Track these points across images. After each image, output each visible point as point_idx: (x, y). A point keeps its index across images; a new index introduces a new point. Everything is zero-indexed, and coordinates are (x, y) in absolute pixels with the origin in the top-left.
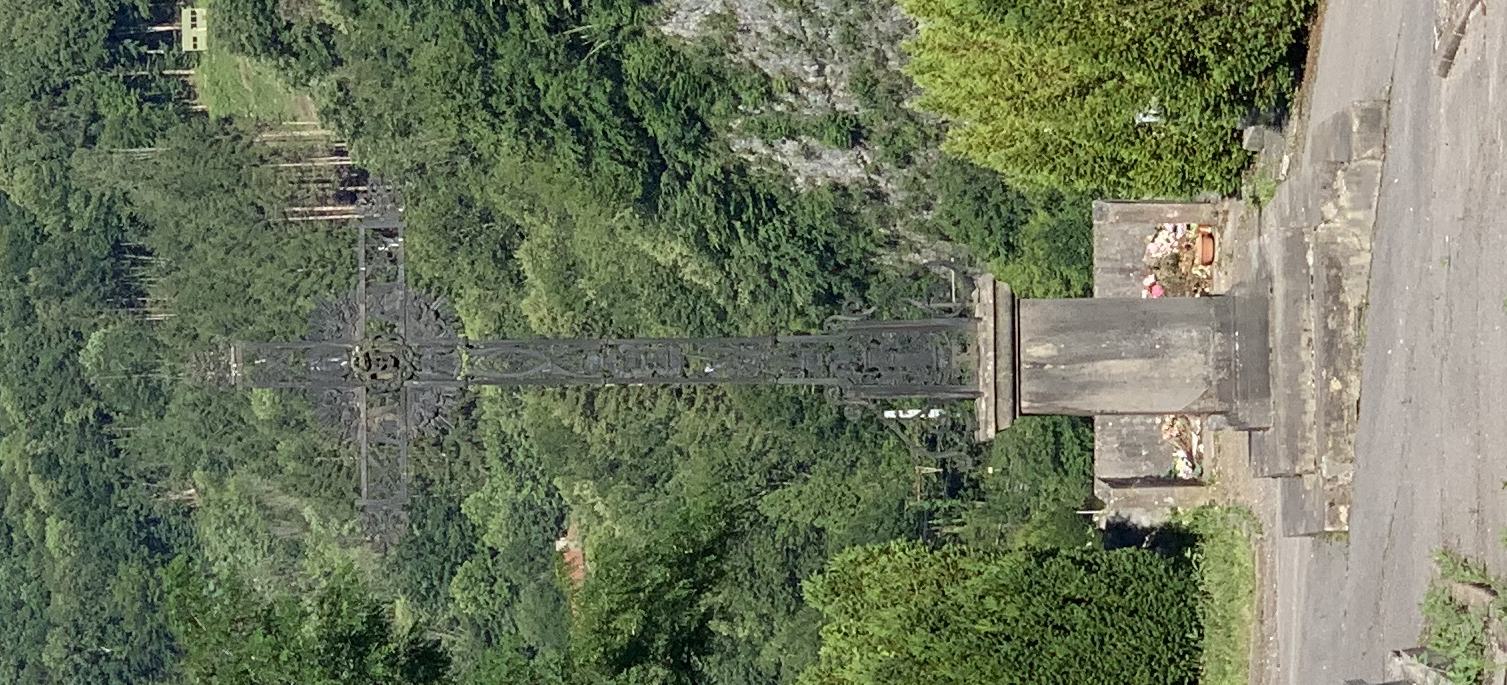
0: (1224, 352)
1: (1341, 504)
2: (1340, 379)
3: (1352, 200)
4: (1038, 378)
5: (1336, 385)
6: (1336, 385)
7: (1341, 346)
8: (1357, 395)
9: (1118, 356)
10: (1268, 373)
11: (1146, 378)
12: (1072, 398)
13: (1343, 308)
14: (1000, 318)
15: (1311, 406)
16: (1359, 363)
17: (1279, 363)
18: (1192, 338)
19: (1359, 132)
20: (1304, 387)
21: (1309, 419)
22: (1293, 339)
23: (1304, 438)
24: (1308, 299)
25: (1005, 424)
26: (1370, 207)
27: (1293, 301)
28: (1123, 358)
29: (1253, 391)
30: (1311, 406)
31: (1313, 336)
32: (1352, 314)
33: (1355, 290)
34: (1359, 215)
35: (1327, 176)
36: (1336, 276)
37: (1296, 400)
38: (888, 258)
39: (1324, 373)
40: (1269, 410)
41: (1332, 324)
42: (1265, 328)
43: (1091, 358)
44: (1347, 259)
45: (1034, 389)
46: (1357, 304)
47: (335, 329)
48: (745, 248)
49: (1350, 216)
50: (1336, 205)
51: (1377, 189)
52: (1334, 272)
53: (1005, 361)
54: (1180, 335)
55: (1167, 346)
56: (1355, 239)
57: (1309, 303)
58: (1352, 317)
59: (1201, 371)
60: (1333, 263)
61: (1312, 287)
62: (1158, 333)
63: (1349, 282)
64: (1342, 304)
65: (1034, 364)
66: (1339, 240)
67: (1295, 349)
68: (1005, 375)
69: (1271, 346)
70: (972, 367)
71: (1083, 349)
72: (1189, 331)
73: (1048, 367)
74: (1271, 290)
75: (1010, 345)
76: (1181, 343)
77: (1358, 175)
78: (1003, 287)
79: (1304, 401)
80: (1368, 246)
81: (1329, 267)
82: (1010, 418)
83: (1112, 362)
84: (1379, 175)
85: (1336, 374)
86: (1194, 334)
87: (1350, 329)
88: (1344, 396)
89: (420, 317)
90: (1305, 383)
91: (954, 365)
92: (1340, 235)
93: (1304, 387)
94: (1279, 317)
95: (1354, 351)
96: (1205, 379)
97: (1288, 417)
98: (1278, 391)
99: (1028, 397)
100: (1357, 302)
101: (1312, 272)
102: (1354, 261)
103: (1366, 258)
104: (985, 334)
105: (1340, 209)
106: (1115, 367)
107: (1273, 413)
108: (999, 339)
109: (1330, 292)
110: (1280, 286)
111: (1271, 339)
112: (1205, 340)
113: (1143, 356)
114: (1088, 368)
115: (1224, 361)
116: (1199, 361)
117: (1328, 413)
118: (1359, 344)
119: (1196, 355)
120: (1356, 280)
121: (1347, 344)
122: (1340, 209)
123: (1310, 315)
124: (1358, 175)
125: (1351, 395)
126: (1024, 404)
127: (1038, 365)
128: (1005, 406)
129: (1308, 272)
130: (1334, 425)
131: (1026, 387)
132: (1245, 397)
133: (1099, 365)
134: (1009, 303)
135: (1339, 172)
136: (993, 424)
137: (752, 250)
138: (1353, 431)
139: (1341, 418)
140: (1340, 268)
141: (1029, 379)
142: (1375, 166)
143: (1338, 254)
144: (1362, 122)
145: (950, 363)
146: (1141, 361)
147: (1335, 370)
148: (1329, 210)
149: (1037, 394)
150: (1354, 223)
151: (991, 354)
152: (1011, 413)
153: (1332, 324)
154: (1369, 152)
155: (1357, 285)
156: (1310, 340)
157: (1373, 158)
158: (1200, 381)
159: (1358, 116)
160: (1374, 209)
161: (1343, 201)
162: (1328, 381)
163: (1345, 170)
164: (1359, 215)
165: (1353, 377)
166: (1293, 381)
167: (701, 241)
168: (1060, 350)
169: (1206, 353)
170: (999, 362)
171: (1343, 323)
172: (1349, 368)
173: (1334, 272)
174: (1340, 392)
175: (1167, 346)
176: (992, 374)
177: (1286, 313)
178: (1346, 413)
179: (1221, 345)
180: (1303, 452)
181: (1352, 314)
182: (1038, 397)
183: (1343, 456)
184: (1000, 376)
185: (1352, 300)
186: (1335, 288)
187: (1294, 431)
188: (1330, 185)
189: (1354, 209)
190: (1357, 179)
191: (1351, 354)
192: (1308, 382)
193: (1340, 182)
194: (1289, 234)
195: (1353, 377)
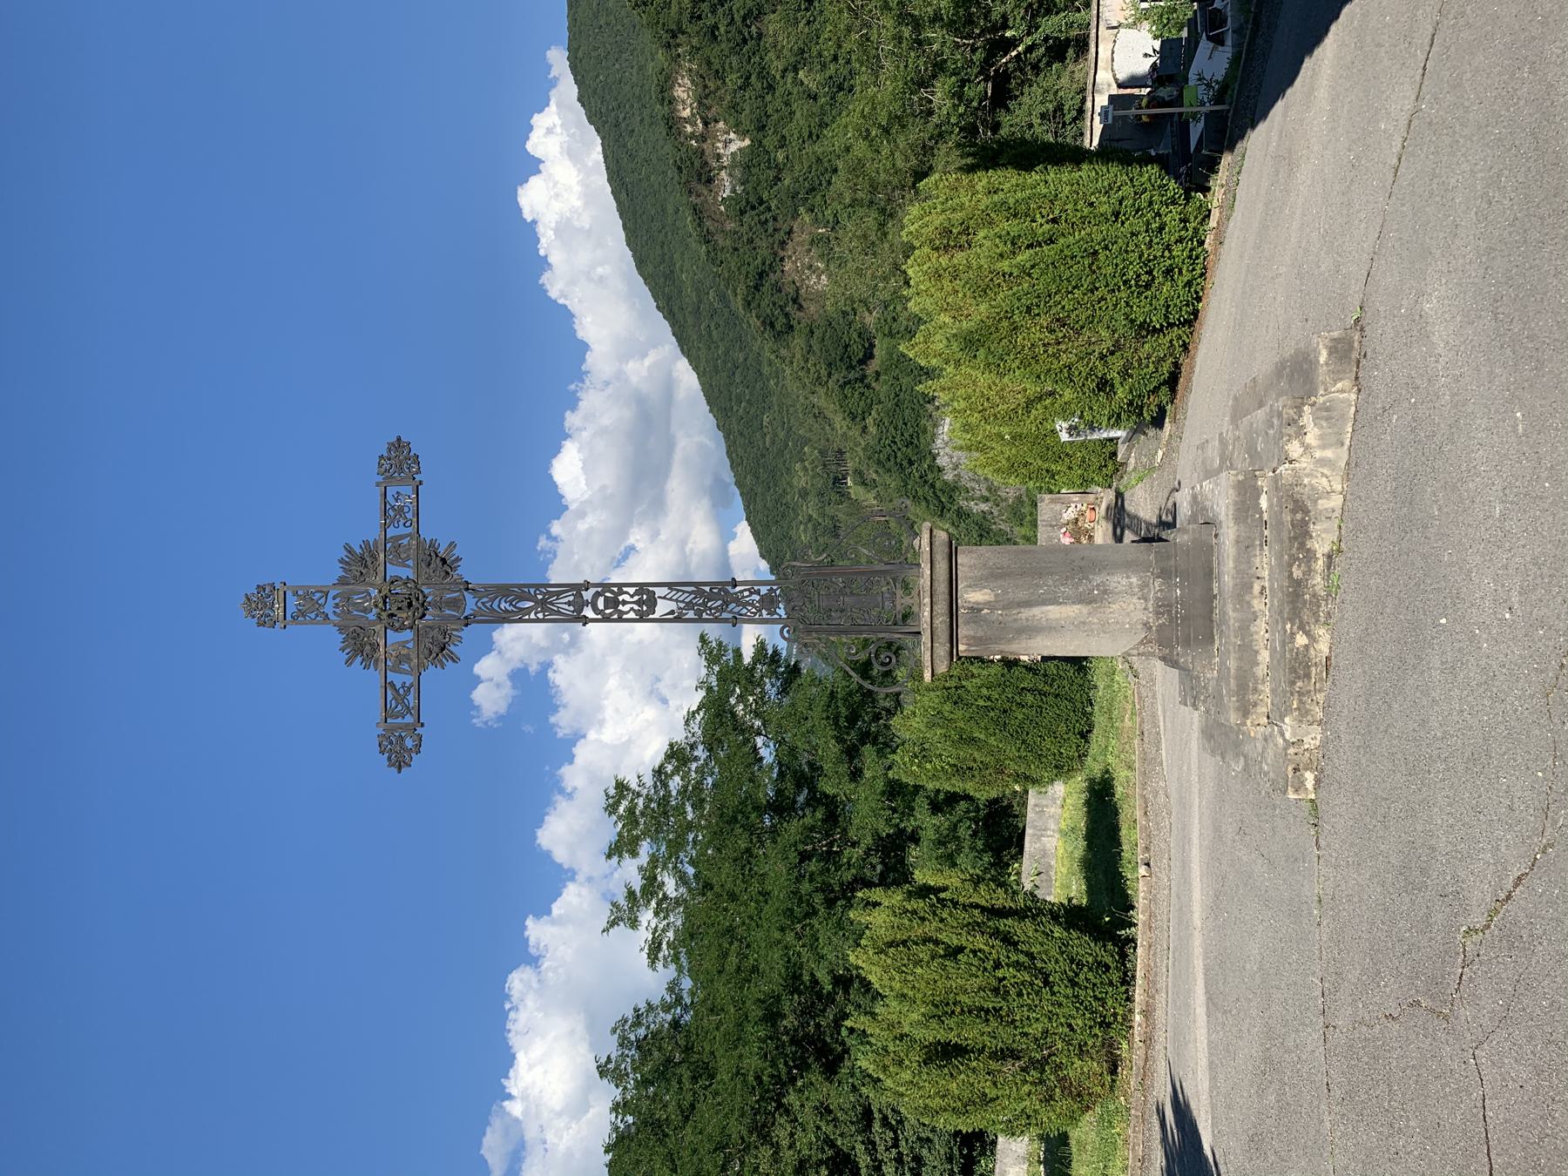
0: (1165, 598)
1: (1306, 770)
2: (1308, 634)
3: (1321, 437)
4: (975, 622)
5: (1301, 640)
6: (1301, 640)
7: (1307, 597)
8: (1326, 651)
9: (1054, 601)
10: (1212, 621)
11: (1084, 623)
12: (1010, 641)
13: (1310, 556)
14: (937, 566)
15: (1264, 657)
16: (1329, 615)
17: (1231, 613)
18: (1131, 584)
19: (1327, 364)
20: (1256, 637)
21: (1261, 671)
22: (1244, 587)
23: (1255, 690)
24: (1261, 545)
25: (942, 668)
26: (1342, 444)
27: (1245, 548)
28: (1061, 603)
29: (1196, 638)
30: (1264, 657)
31: (1267, 585)
32: (1320, 562)
33: (1323, 535)
34: (1329, 454)
35: (1291, 412)
36: (1303, 519)
37: (1247, 652)
39: (1288, 626)
40: (1214, 657)
41: (1297, 573)
42: (1209, 574)
43: (1028, 604)
44: (1315, 502)
45: (972, 633)
46: (1326, 551)
47: (358, 574)
49: (1318, 454)
50: (1302, 444)
51: (1350, 424)
52: (1299, 516)
53: (942, 607)
54: (1119, 581)
55: (1105, 592)
56: (1324, 479)
57: (1262, 549)
58: (1320, 564)
59: (1141, 616)
60: (1299, 506)
61: (1266, 533)
62: (1098, 580)
63: (1317, 527)
64: (1309, 550)
65: (972, 608)
66: (1306, 481)
67: (1247, 598)
68: (941, 621)
69: (1215, 592)
70: (915, 609)
71: (1022, 595)
72: (1128, 577)
73: (985, 611)
74: (1216, 536)
75: (947, 591)
76: (1120, 588)
77: (1327, 409)
78: (942, 536)
79: (1257, 652)
80: (1339, 488)
81: (1294, 511)
82: (946, 663)
83: (1050, 607)
84: (1353, 409)
85: (1302, 628)
86: (1134, 580)
87: (1318, 579)
88: (1312, 652)
89: (429, 564)
90: (1257, 633)
91: (899, 607)
92: (1308, 475)
93: (1256, 637)
94: (1230, 564)
95: (1323, 603)
96: (1145, 625)
97: (1239, 668)
99: (965, 641)
100: (1326, 549)
101: (1265, 516)
102: (1323, 504)
103: (1336, 501)
105: (1307, 448)
106: (1054, 612)
107: (1217, 659)
108: (936, 584)
109: (1295, 538)
110: (1229, 534)
111: (1215, 585)
112: (1144, 586)
113: (1081, 602)
114: (1026, 613)
115: (1164, 607)
116: (1138, 606)
117: (1293, 670)
118: (1329, 595)
119: (1135, 600)
120: (1325, 526)
121: (1314, 595)
122: (1307, 448)
123: (1264, 563)
124: (1327, 409)
125: (1321, 651)
126: (961, 647)
127: (975, 609)
128: (942, 650)
129: (1261, 517)
130: (1299, 684)
131: (963, 631)
132: (1187, 643)
134: (947, 550)
135: (1306, 408)
136: (930, 669)
138: (1320, 691)
139: (1308, 676)
140: (1306, 512)
141: (967, 623)
142: (1348, 400)
143: (1305, 497)
144: (1330, 354)
145: (895, 606)
146: (1078, 606)
147: (1301, 622)
148: (1294, 449)
149: (974, 637)
150: (1322, 462)
151: (927, 600)
152: (947, 656)
153: (1297, 573)
154: (1339, 385)
155: (1325, 531)
156: (1263, 588)
157: (1343, 391)
158: (1140, 627)
159: (1326, 347)
160: (1346, 447)
161: (1310, 439)
162: (1293, 634)
163: (1312, 405)
164: (1329, 454)
165: (1321, 631)
166: (1245, 629)
167: (953, 524)
168: (996, 595)
169: (1146, 600)
170: (935, 607)
171: (1309, 572)
172: (1317, 621)
173: (1299, 516)
174: (1306, 647)
175: (1105, 592)
176: (929, 620)
177: (1237, 560)
178: (1313, 669)
179: (1161, 590)
180: (1255, 705)
181: (1320, 562)
183: (1309, 718)
184: (937, 622)
185: (1321, 544)
186: (1301, 533)
187: (1245, 686)
188: (1295, 422)
189: (1323, 447)
190: (1326, 413)
191: (1319, 606)
192: (1261, 629)
193: (1307, 418)
194: (1241, 478)
195: (1321, 631)
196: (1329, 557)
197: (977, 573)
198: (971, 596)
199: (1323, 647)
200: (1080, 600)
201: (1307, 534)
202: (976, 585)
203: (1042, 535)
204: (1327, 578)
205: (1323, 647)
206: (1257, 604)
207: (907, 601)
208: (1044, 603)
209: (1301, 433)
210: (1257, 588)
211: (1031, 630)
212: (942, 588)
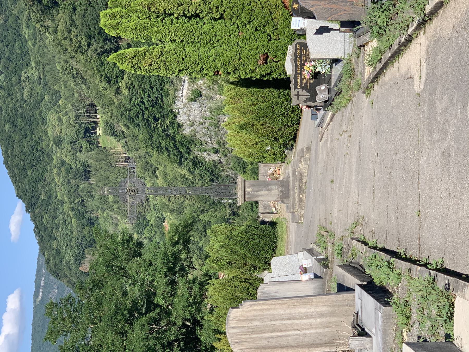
3: (304, 163)
5: (301, 196)
6: (301, 196)
9: (263, 191)
13: (302, 182)
15: (297, 200)
16: (305, 192)
17: (291, 192)
21: (296, 202)
22: (294, 188)
25: (243, 202)
27: (294, 181)
30: (297, 200)
34: (305, 166)
37: (294, 199)
38: (222, 174)
41: (300, 185)
42: (289, 186)
43: (258, 191)
48: (197, 171)
53: (243, 191)
54: (274, 187)
59: (278, 193)
62: (270, 187)
68: (243, 194)
71: (257, 189)
85: (301, 194)
98: (291, 197)
103: (306, 174)
104: (239, 187)
105: (302, 165)
106: (262, 193)
110: (291, 178)
113: (267, 191)
114: (257, 193)
115: (281, 192)
117: (300, 201)
122: (302, 165)
123: (297, 184)
128: (243, 200)
131: (246, 196)
132: (285, 198)
133: (259, 192)
137: (198, 171)
139: (302, 202)
146: (267, 192)
148: (300, 165)
150: (304, 167)
161: (303, 164)
164: (305, 166)
165: (304, 195)
166: (294, 195)
167: (189, 170)
169: (278, 190)
171: (302, 185)
182: (248, 198)
185: (304, 181)
186: (301, 179)
187: (294, 205)
189: (305, 165)
190: (305, 160)
192: (296, 195)
193: (302, 160)
195: (304, 195)
196: (305, 183)
197: (249, 185)
198: (248, 190)
199: (304, 197)
200: (267, 190)
201: (302, 179)
202: (248, 188)
203: (260, 178)
204: (305, 186)
205: (304, 197)
206: (296, 191)
207: (235, 191)
208: (261, 191)
209: (301, 162)
210: (296, 188)
211: (258, 196)
212: (243, 188)
